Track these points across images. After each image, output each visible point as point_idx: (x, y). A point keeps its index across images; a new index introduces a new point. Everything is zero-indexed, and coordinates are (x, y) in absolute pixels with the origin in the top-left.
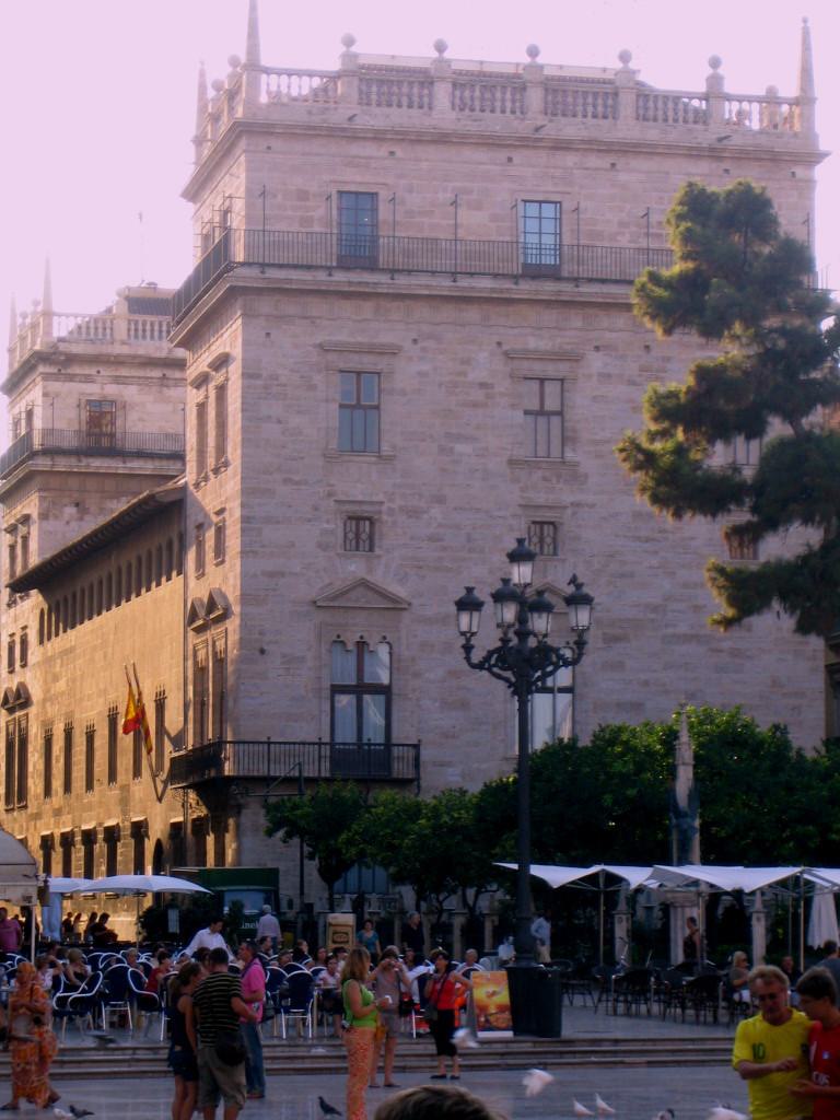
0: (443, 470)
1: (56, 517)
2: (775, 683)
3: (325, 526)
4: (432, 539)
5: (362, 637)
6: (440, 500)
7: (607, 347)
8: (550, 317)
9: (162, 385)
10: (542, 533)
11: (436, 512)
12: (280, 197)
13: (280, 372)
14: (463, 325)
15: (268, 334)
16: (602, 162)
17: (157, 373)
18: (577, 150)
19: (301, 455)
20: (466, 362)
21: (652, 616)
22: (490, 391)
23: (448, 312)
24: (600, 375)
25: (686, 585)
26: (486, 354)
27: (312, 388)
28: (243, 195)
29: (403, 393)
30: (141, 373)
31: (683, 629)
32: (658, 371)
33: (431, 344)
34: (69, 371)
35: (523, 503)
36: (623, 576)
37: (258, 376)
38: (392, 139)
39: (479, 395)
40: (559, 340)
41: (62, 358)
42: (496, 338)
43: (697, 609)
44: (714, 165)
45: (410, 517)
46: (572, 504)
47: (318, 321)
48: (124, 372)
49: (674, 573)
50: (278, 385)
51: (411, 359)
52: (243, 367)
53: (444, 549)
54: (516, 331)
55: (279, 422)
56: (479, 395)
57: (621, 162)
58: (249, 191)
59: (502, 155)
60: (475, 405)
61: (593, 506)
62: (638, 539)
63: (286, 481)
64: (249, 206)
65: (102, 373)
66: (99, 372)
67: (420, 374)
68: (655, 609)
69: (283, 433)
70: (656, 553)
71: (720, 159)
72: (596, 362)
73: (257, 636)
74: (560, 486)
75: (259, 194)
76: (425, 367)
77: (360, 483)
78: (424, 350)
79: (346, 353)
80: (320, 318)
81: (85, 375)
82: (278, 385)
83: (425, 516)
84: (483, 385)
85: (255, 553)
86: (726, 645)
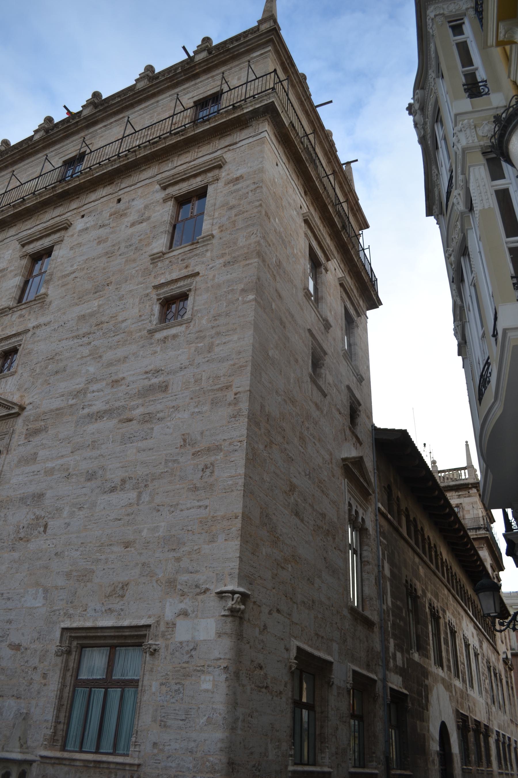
2: (186, 441)
25: (110, 364)
31: (99, 406)
32: (123, 211)
72: (79, 224)
86: (140, 410)
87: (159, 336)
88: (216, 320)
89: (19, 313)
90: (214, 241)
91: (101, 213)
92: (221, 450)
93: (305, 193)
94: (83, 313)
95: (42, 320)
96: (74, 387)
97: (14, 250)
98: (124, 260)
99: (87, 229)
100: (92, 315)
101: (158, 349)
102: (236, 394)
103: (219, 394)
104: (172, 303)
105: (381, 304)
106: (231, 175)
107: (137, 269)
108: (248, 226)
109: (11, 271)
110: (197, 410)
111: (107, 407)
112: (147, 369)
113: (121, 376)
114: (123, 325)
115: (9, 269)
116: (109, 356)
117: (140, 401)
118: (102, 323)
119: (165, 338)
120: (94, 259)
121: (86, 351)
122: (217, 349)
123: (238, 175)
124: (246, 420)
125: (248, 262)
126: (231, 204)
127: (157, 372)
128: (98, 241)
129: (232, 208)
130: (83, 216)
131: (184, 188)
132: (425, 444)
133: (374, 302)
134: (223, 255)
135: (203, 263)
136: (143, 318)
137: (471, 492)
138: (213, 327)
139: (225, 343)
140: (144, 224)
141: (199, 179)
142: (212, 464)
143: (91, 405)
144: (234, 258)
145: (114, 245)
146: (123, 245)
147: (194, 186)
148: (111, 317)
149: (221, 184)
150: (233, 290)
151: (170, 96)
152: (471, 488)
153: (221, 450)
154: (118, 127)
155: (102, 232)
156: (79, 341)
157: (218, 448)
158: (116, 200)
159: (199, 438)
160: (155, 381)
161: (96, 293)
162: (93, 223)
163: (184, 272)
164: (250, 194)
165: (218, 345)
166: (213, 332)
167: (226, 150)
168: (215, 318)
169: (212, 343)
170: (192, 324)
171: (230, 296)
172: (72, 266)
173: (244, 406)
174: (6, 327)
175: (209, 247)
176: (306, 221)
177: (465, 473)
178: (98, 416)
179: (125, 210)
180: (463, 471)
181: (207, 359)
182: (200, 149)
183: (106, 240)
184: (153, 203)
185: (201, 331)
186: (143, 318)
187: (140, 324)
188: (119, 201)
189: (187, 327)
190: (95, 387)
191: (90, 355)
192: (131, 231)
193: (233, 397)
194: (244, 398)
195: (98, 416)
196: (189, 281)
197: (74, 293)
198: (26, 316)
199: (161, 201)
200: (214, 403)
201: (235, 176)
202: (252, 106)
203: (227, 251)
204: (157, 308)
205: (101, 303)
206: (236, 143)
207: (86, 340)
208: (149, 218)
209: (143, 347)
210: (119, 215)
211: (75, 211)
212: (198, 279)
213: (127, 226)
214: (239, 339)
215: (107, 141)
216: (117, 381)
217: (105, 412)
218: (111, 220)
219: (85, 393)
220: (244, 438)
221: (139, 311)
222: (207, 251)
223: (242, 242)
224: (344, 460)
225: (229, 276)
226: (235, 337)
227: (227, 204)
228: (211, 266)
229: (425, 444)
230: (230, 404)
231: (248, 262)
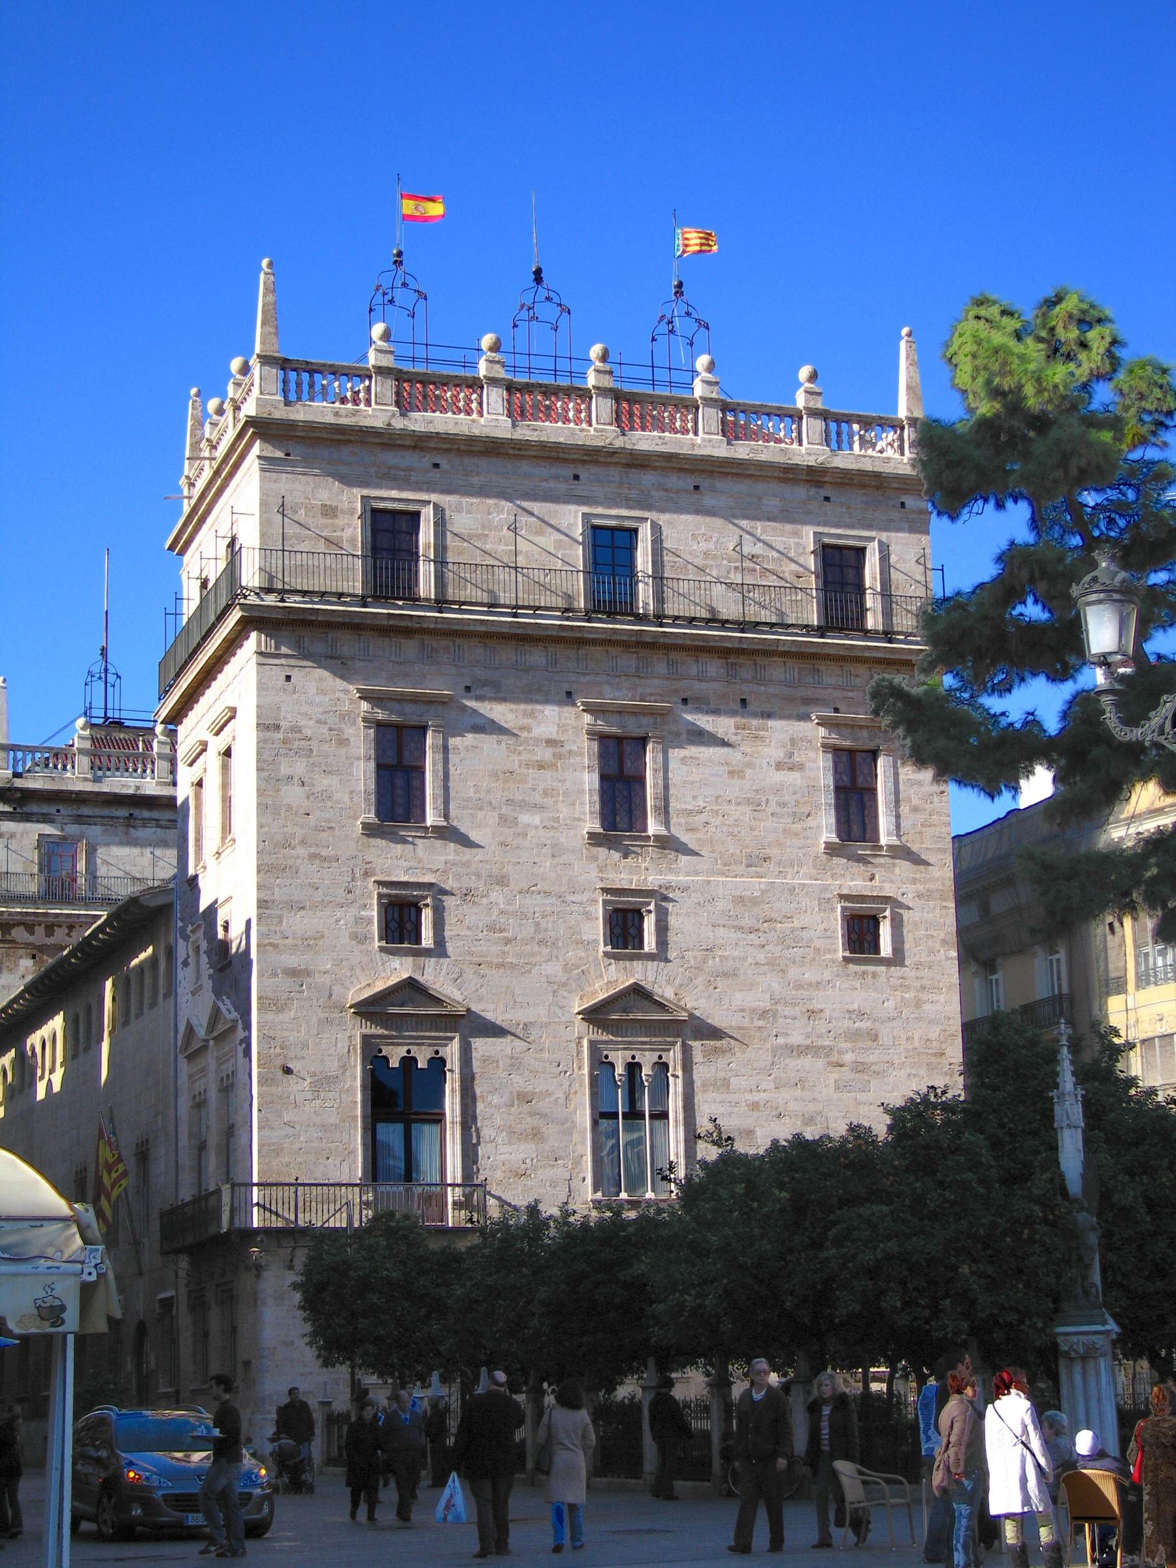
0: (504, 844)
1: (10, 970)
4: (492, 928)
5: (409, 1052)
6: (502, 881)
9: (128, 826)
10: (625, 924)
11: (497, 895)
13: (302, 723)
14: (526, 671)
15: (288, 678)
16: (690, 481)
17: (123, 812)
18: (655, 468)
19: (331, 825)
21: (761, 1023)
22: (558, 750)
23: (507, 653)
27: (343, 742)
28: (255, 508)
30: (105, 812)
31: (797, 1039)
34: (26, 809)
36: (725, 975)
37: (278, 727)
38: (435, 449)
41: (18, 795)
42: (566, 687)
43: (812, 1013)
44: (813, 491)
47: (350, 663)
48: (86, 811)
50: (300, 739)
52: (258, 717)
53: (508, 941)
56: (546, 754)
58: (264, 504)
59: (568, 471)
60: (541, 766)
61: (686, 889)
62: (740, 928)
63: (313, 856)
64: (265, 524)
65: (63, 811)
66: (58, 811)
68: (764, 1014)
69: (308, 798)
71: (819, 484)
73: (278, 1051)
75: (277, 509)
77: (409, 862)
80: (352, 659)
81: (43, 814)
82: (300, 739)
83: (484, 901)
84: (550, 742)
85: (275, 946)
87: (852, 967)
100: (755, 902)
101: (858, 985)
103: (933, 1060)
107: (804, 851)
110: (913, 1072)
111: (808, 1042)
113: (817, 1007)
115: (567, 747)
117: (849, 1045)
126: (914, 803)
127: (862, 1014)
128: (727, 769)
134: (914, 881)
135: (891, 882)
140: (797, 775)
143: (786, 1034)
145: (757, 791)
146: (773, 799)
148: (785, 917)
161: (749, 866)
171: (930, 943)
172: (695, 798)
174: (606, 866)
178: (800, 1051)
190: (787, 1011)
192: (778, 777)
197: (713, 851)
217: (808, 1047)
218: (739, 737)
219: (774, 1016)
226: (942, 998)
231: (945, 904)
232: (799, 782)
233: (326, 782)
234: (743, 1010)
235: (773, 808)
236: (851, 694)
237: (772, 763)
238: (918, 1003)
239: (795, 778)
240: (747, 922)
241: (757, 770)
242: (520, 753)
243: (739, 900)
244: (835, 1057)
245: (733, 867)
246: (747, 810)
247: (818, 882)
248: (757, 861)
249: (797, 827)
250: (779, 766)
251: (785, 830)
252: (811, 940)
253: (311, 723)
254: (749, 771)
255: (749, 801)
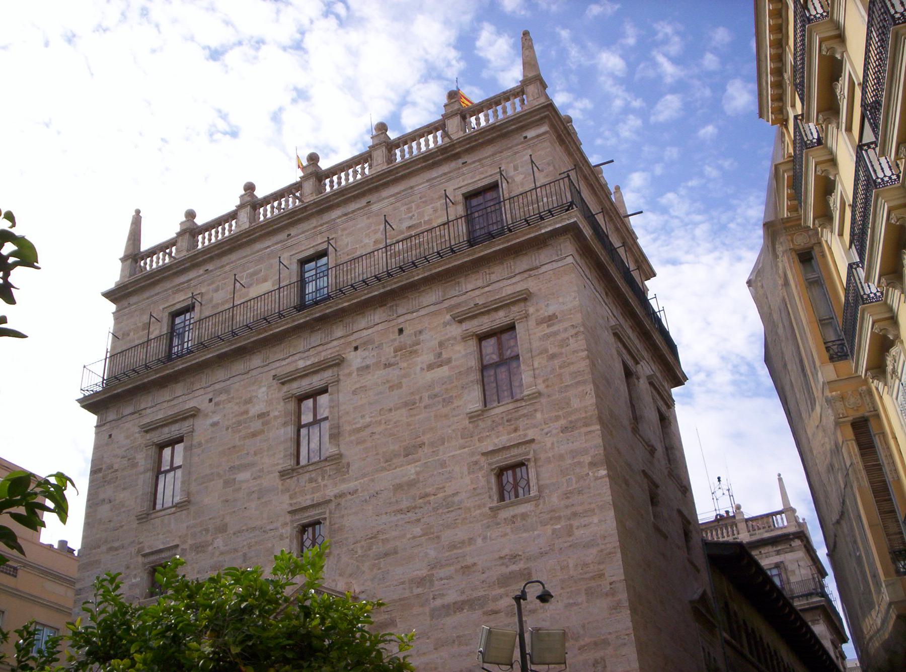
3: (134, 581)
6: (222, 529)
7: (365, 343)
8: (316, 338)
11: (219, 542)
12: (132, 334)
15: (110, 436)
16: (363, 202)
20: (249, 401)
21: (420, 590)
24: (358, 369)
25: (453, 546)
26: (264, 389)
29: (200, 444)
31: (452, 597)
33: (223, 397)
35: (290, 509)
36: (386, 555)
39: (257, 425)
40: (323, 354)
42: (273, 373)
43: (466, 569)
45: (198, 553)
46: (335, 497)
49: (438, 537)
51: (206, 415)
54: (287, 361)
55: (110, 501)
56: (257, 425)
57: (373, 198)
59: (282, 236)
60: (254, 435)
61: (356, 491)
62: (400, 511)
63: (111, 549)
67: (215, 424)
68: (421, 582)
70: (418, 520)
71: (457, 156)
72: (355, 359)
74: (325, 482)
76: (216, 419)
78: (217, 404)
79: (160, 430)
83: (210, 548)
84: (261, 416)
87: (505, 514)
88: (568, 498)
89: (307, 476)
90: (543, 400)
91: (380, 346)
92: (609, 644)
93: (606, 294)
94: (397, 481)
95: (344, 487)
96: (415, 573)
97: (269, 387)
98: (432, 414)
99: (368, 367)
100: (412, 484)
101: (508, 530)
102: (611, 584)
103: (593, 584)
104: (509, 476)
105: (686, 379)
106: (542, 312)
108: (578, 383)
109: (276, 417)
111: (464, 597)
112: (503, 554)
113: (469, 561)
114: (456, 499)
115: (272, 415)
116: (448, 536)
117: (502, 591)
118: (427, 495)
119: (513, 517)
120: (391, 410)
121: (417, 530)
122: (578, 533)
123: (550, 313)
124: (629, 612)
125: (589, 429)
127: (514, 558)
128: (387, 385)
129: (553, 357)
130: (356, 348)
131: (485, 324)
132: (719, 478)
133: (678, 379)
134: (557, 418)
135: (535, 426)
136: (478, 491)
137: (793, 544)
138: (567, 507)
139: (585, 526)
141: (501, 313)
142: (603, 659)
143: (443, 595)
144: (571, 422)
145: (412, 394)
146: (426, 395)
147: (498, 322)
149: (532, 323)
150: (579, 463)
151: (427, 181)
152: (792, 540)
153: (609, 644)
154: (365, 217)
155: (393, 374)
156: (402, 516)
157: (605, 643)
158: (397, 331)
159: (582, 632)
160: (514, 568)
161: (407, 455)
162: (374, 360)
163: (515, 438)
164: (571, 341)
165: (578, 528)
166: (569, 512)
167: (526, 275)
168: (567, 495)
169: (571, 526)
170: (541, 501)
172: (363, 417)
173: (623, 596)
174: (296, 493)
175: (537, 406)
176: (616, 335)
177: (782, 519)
178: (458, 607)
179: (414, 345)
180: (778, 516)
181: (569, 544)
182: (492, 270)
183: (399, 386)
184: (448, 340)
185: (554, 511)
186: (478, 491)
187: (477, 498)
188: (401, 331)
189: (537, 506)
190: (442, 573)
191: (424, 535)
192: (429, 376)
193: (608, 587)
194: (621, 587)
195: (458, 607)
196: (522, 450)
197: (377, 454)
198: (320, 480)
199: (459, 338)
200: (590, 593)
201: (546, 314)
202: (550, 225)
203: (560, 413)
204: (493, 480)
205: (418, 469)
206: (537, 268)
207: (411, 516)
208: (449, 361)
209: (488, 527)
210: (408, 351)
211: (342, 341)
212: (534, 446)
213: (422, 369)
214: (600, 521)
215: (360, 241)
216: (467, 567)
217: (464, 602)
218: (397, 358)
219: (431, 581)
220: (631, 631)
221: (472, 483)
222: (536, 411)
223: (575, 403)
224: (691, 602)
225: (570, 444)
226: (595, 520)
227: (546, 351)
228: (546, 431)
229: (719, 478)
230: (607, 595)
231: (589, 429)
232: (447, 373)
233: (122, 496)
234: (403, 583)
235: (426, 401)
236: (487, 289)
237: (425, 367)
238: (570, 531)
239: (444, 371)
240: (404, 505)
241: (413, 376)
242: (240, 431)
243: (398, 488)
244: (491, 606)
245: (395, 461)
246: (404, 411)
247: (466, 449)
248: (409, 452)
249: (445, 410)
250: (430, 367)
251: (436, 416)
252: (461, 502)
253: (119, 460)
254: (404, 380)
255: (406, 404)
